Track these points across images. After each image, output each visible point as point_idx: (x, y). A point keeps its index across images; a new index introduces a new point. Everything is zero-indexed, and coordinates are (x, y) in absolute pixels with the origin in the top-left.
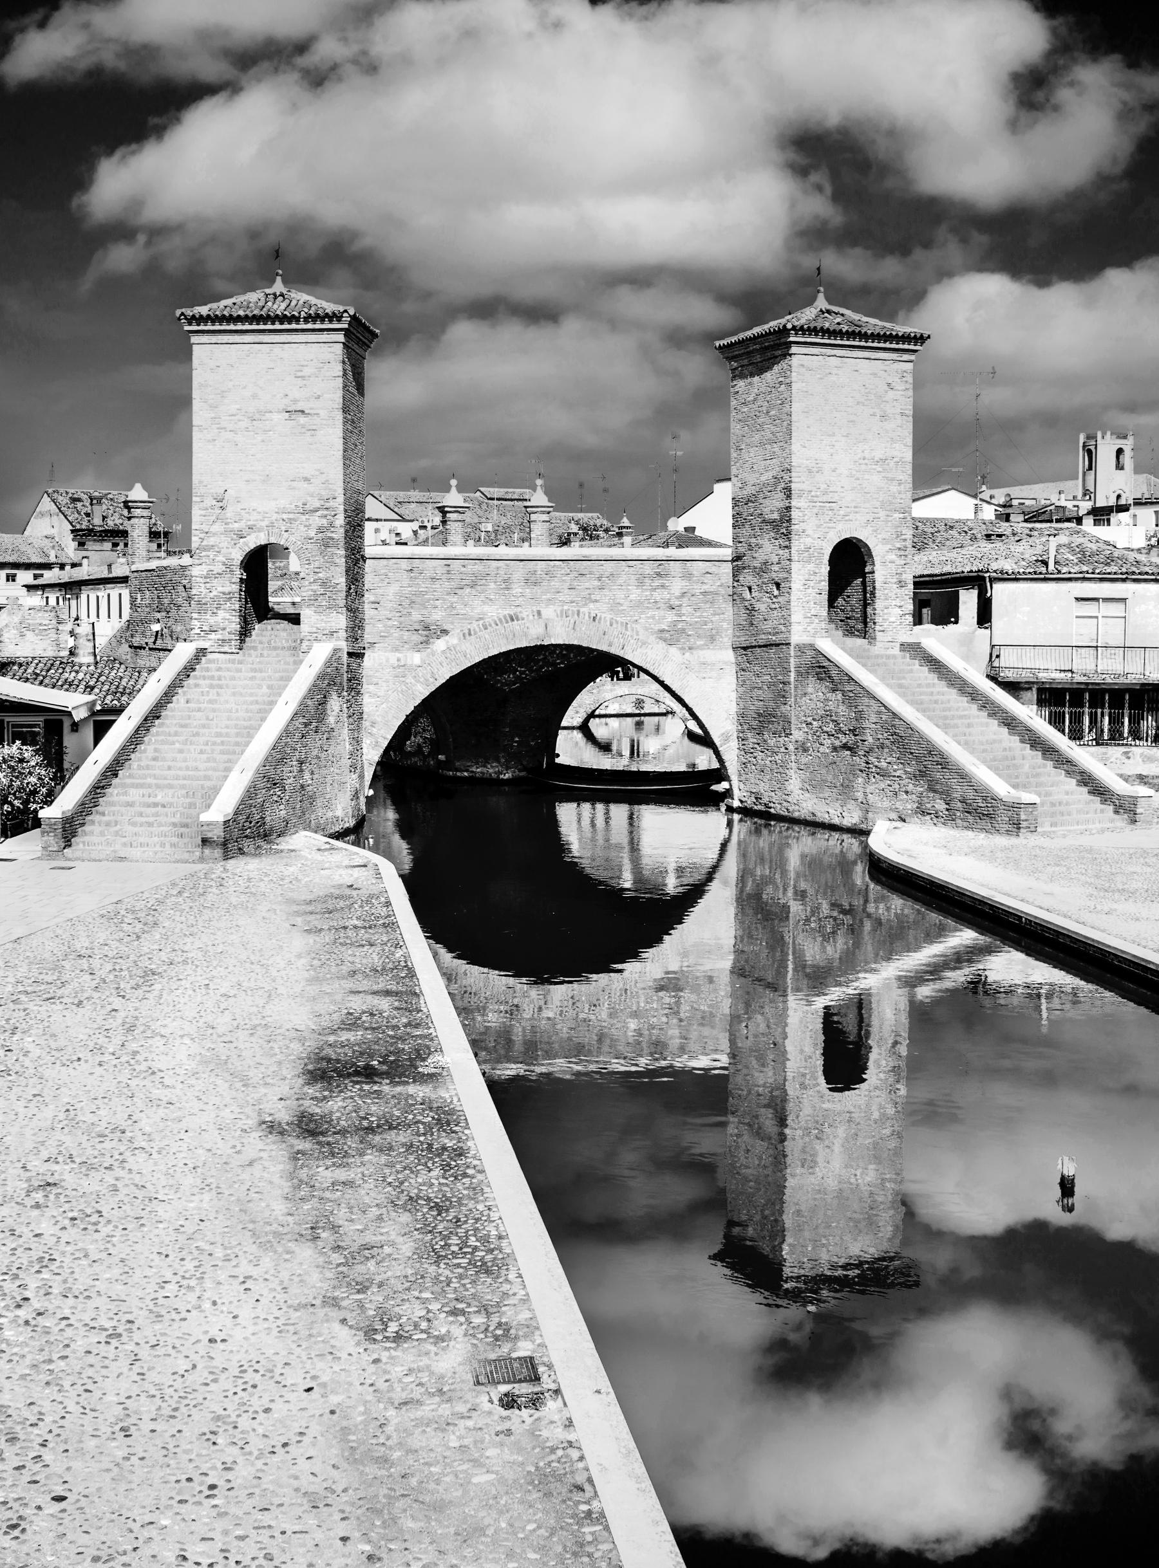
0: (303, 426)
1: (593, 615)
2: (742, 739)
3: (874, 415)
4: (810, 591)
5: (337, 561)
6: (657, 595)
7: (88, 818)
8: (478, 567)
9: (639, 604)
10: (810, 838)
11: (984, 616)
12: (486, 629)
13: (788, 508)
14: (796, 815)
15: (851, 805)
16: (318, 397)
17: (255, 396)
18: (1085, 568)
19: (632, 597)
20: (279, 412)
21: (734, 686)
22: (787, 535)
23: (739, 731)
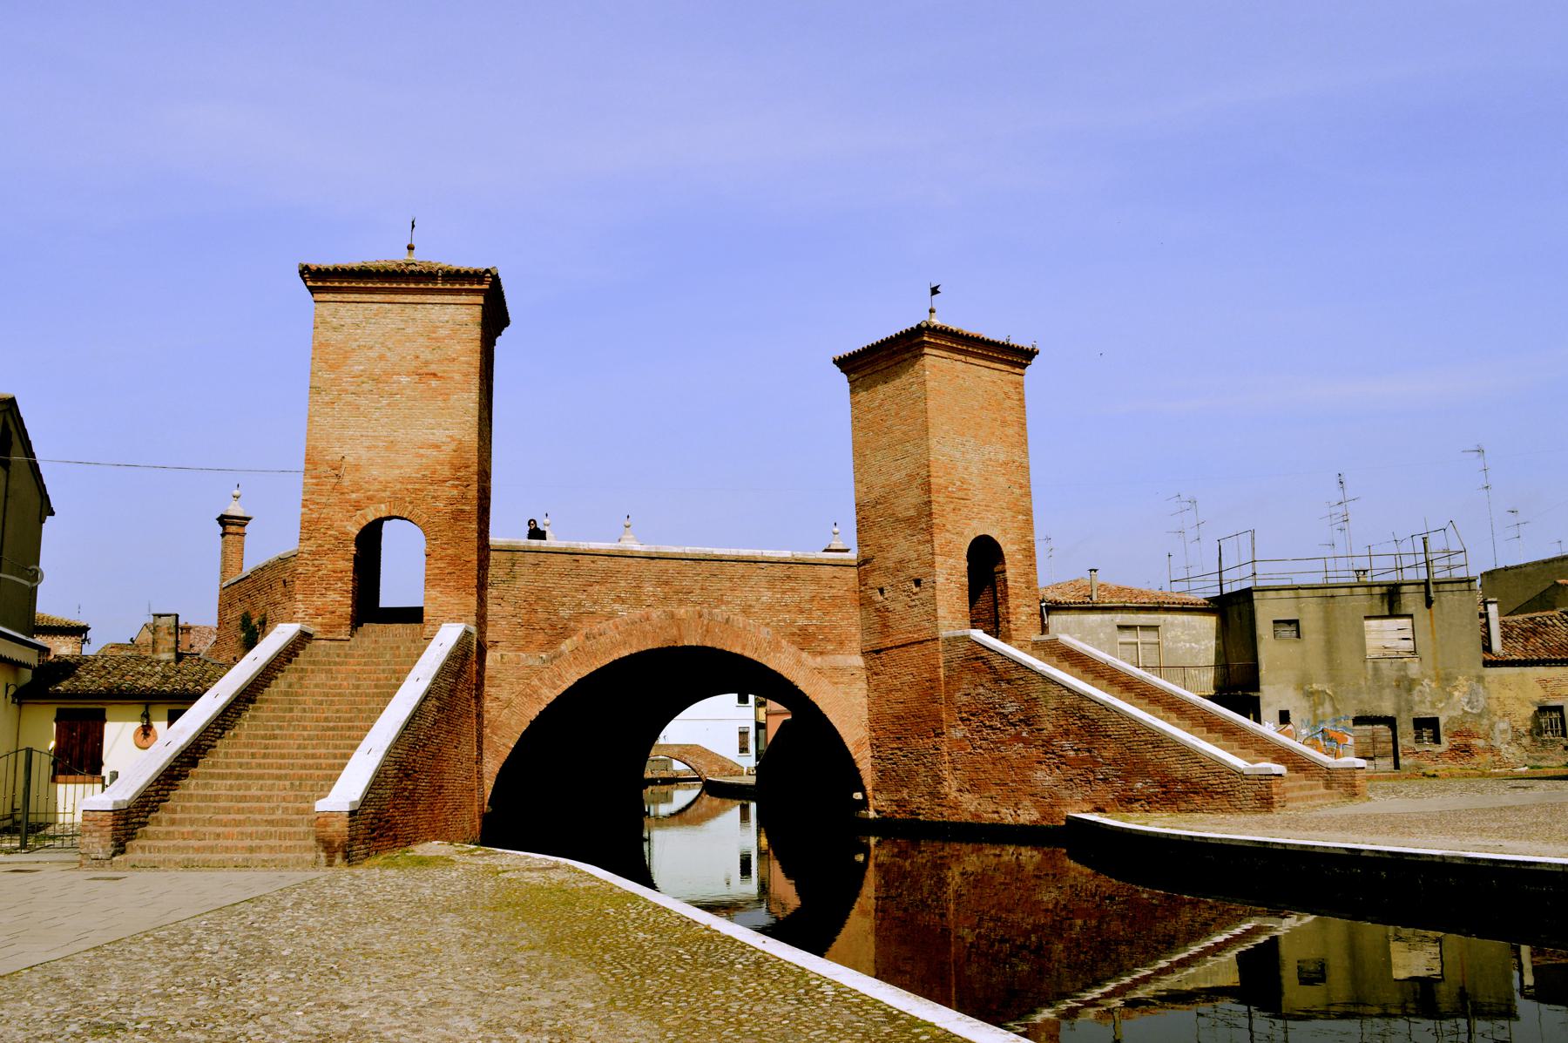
0: (435, 390)
3: (995, 420)
4: (952, 584)
5: (469, 536)
6: (787, 598)
7: (153, 815)
9: (770, 607)
13: (930, 502)
16: (454, 360)
17: (382, 357)
20: (408, 375)
22: (929, 530)
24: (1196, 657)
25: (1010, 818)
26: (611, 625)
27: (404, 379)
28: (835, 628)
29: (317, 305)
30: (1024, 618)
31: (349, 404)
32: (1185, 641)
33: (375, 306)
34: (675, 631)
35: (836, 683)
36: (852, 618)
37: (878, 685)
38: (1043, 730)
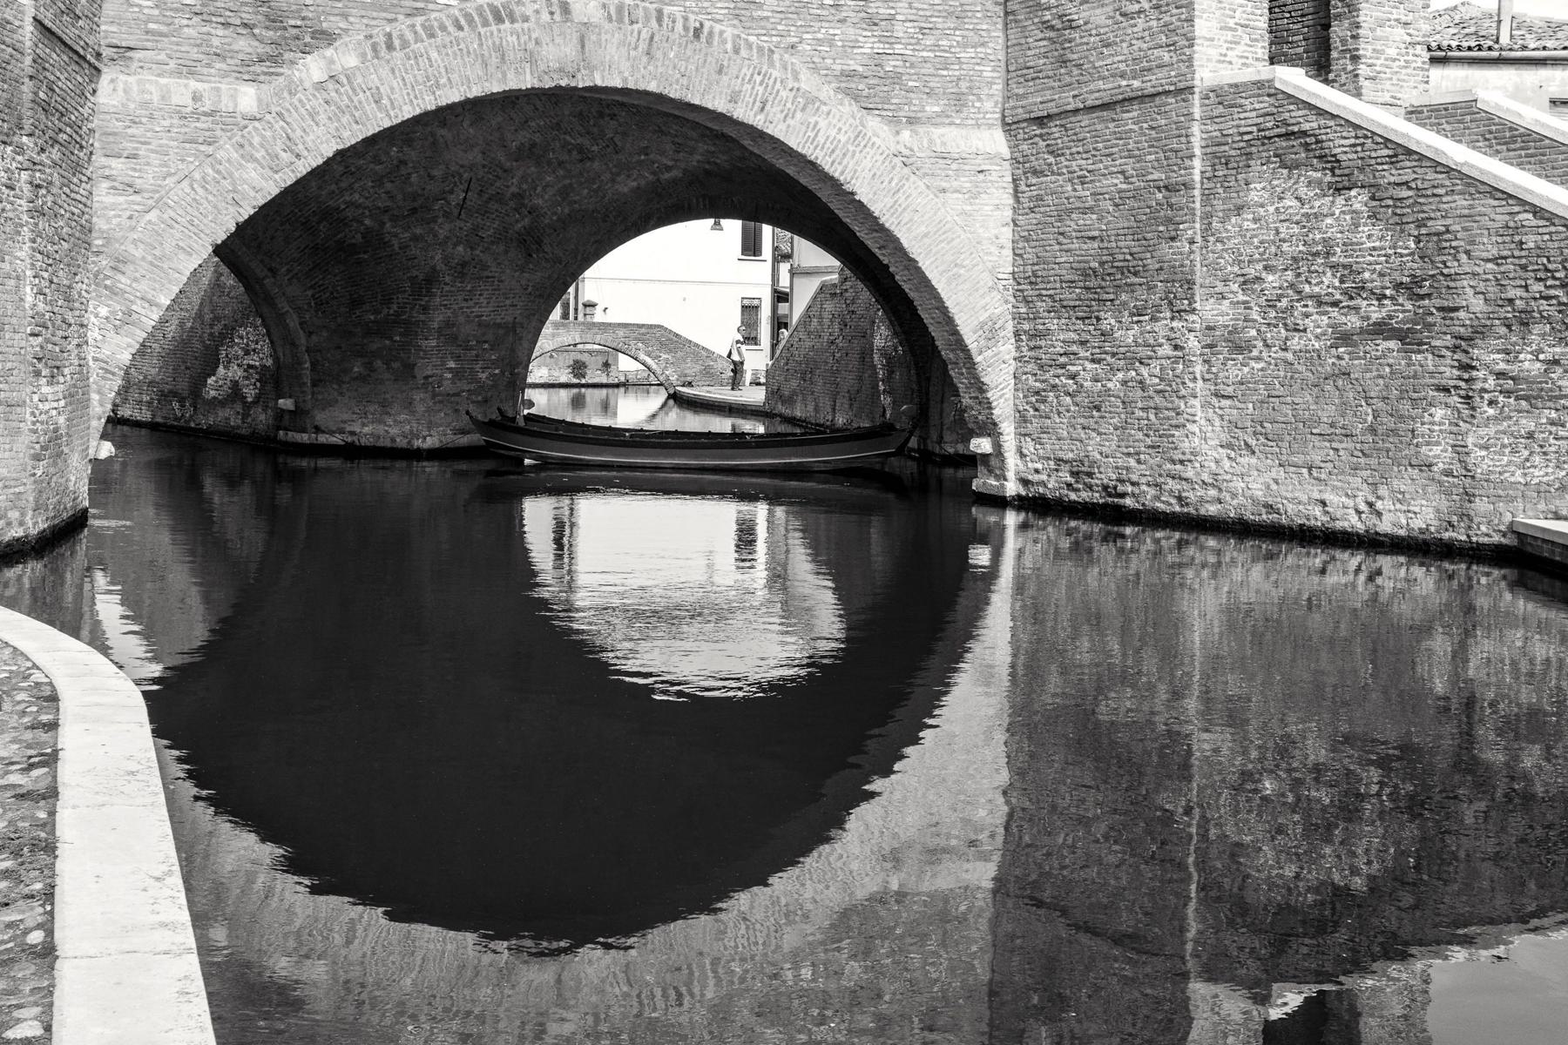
1: (693, 24)
2: (1030, 336)
10: (1257, 571)
12: (432, 36)
14: (1212, 510)
15: (1405, 481)
21: (1009, 213)
23: (1017, 317)
25: (1354, 519)
26: (419, 28)
30: (1392, 52)
34: (569, 50)
35: (944, 191)
36: (983, 45)
37: (1040, 198)
38: (1456, 309)
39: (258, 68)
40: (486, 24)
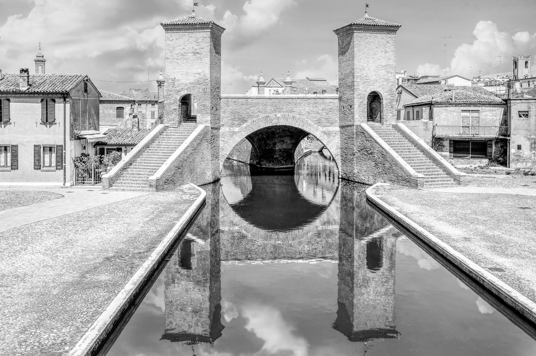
0: (198, 57)
1: (293, 116)
3: (382, 51)
6: (314, 109)
8: (257, 101)
11: (431, 117)
13: (354, 81)
17: (184, 48)
18: (465, 100)
19: (306, 110)
24: (495, 122)
27: (190, 54)
28: (330, 119)
29: (166, 34)
30: (389, 117)
31: (176, 62)
32: (490, 116)
33: (181, 33)
34: (277, 121)
39: (238, 126)
40: (265, 118)
